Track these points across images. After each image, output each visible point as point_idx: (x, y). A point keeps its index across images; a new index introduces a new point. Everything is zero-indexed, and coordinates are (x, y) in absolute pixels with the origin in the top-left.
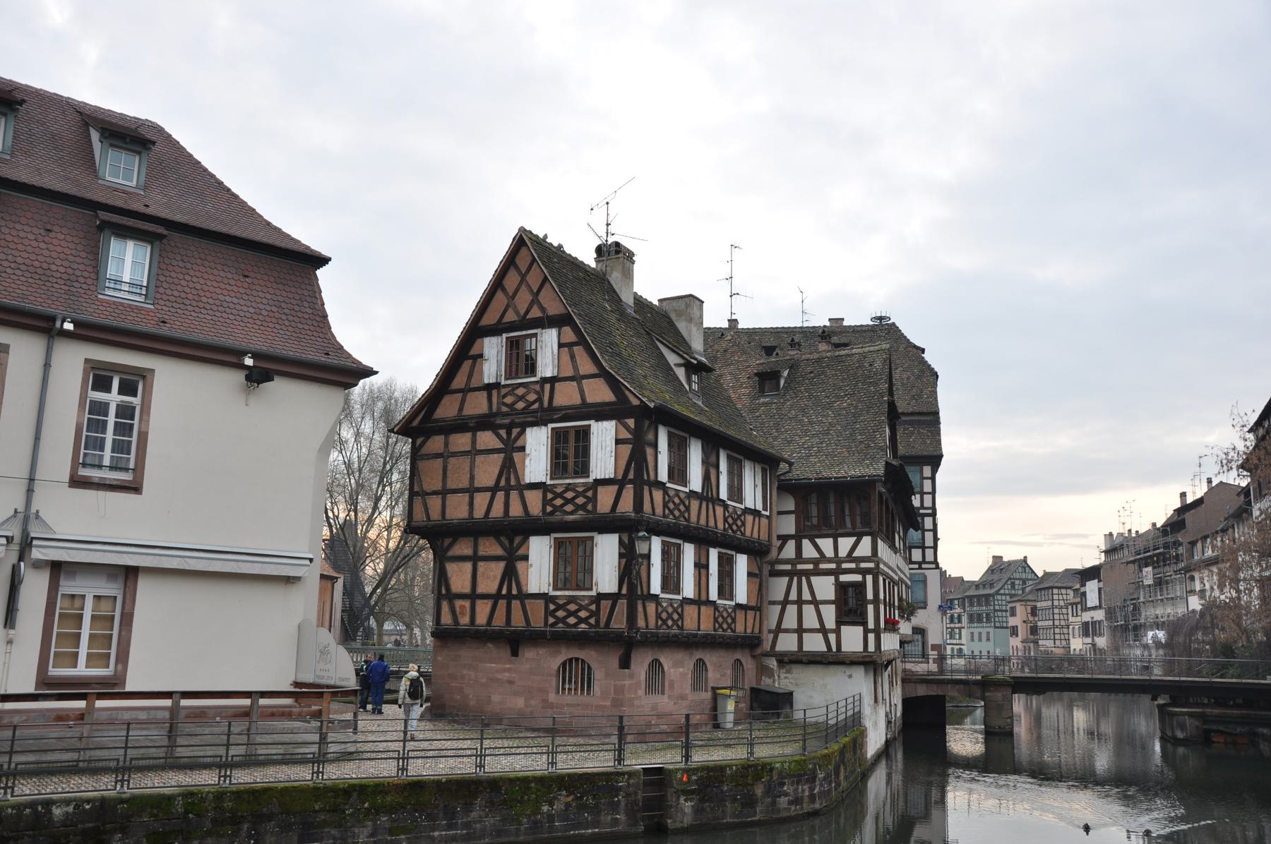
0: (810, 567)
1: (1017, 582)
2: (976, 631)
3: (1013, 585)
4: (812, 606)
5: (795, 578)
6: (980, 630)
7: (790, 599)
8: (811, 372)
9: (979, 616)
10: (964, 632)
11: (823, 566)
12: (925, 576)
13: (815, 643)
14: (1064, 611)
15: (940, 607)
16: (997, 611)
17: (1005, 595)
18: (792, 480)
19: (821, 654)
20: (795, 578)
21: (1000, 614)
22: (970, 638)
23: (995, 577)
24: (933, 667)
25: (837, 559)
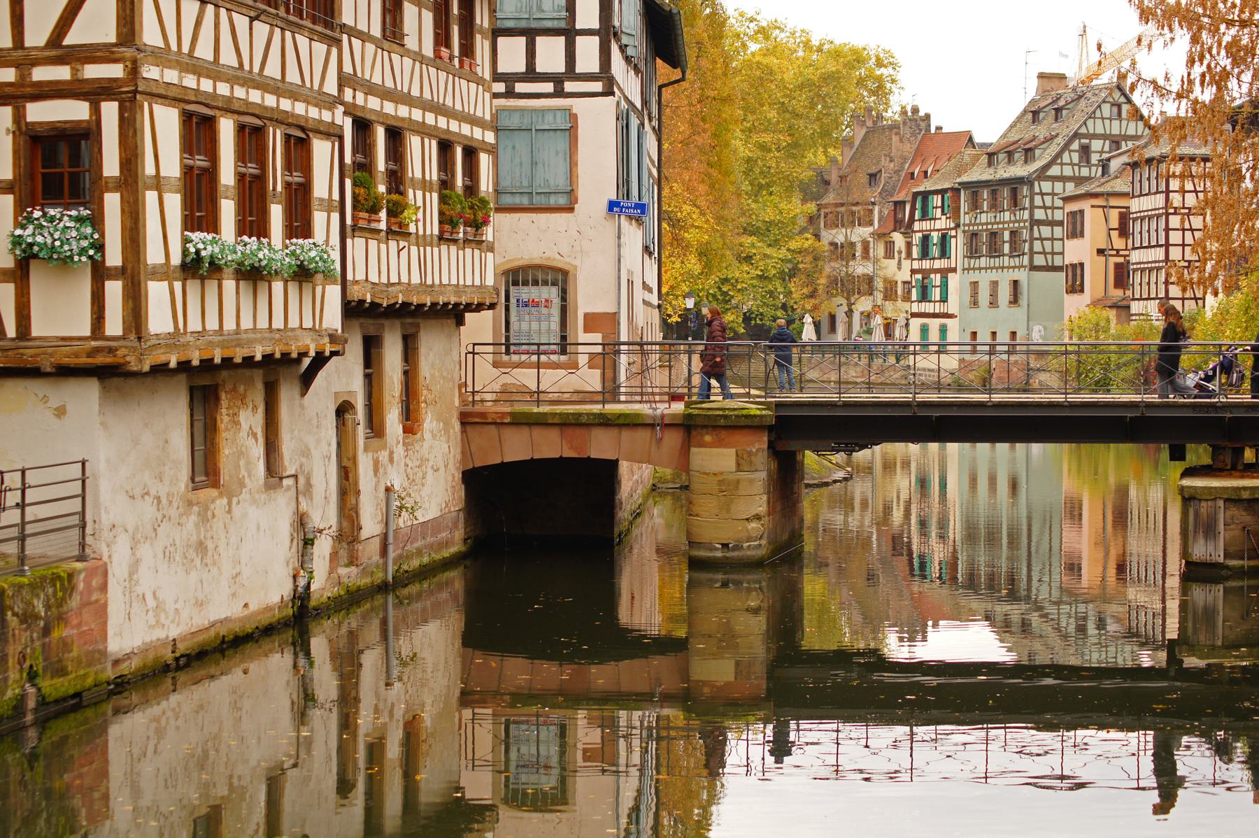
1: (1096, 145)
2: (984, 279)
3: (1085, 151)
6: (994, 275)
9: (993, 235)
10: (953, 280)
12: (574, 118)
15: (612, 205)
16: (1040, 223)
17: (1063, 179)
21: (1046, 231)
23: (1041, 131)
24: (592, 380)
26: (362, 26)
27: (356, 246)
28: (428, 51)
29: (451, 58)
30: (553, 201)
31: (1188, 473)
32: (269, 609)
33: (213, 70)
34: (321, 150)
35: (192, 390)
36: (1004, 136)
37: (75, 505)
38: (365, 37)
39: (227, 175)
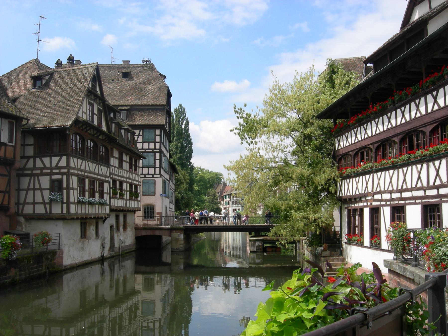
0: (39, 172)
4: (40, 191)
5: (33, 177)
7: (30, 188)
8: (59, 77)
9: (236, 202)
11: (45, 171)
12: (155, 181)
13: (40, 210)
15: (161, 195)
18: (30, 128)
19: (43, 215)
20: (33, 177)
25: (51, 168)
26: (115, 165)
27: (113, 200)
28: (128, 169)
29: (132, 171)
30: (152, 194)
31: (251, 237)
32: (96, 258)
33: (85, 171)
34: (106, 185)
35: (81, 223)
37: (58, 241)
38: (115, 167)
39: (87, 187)
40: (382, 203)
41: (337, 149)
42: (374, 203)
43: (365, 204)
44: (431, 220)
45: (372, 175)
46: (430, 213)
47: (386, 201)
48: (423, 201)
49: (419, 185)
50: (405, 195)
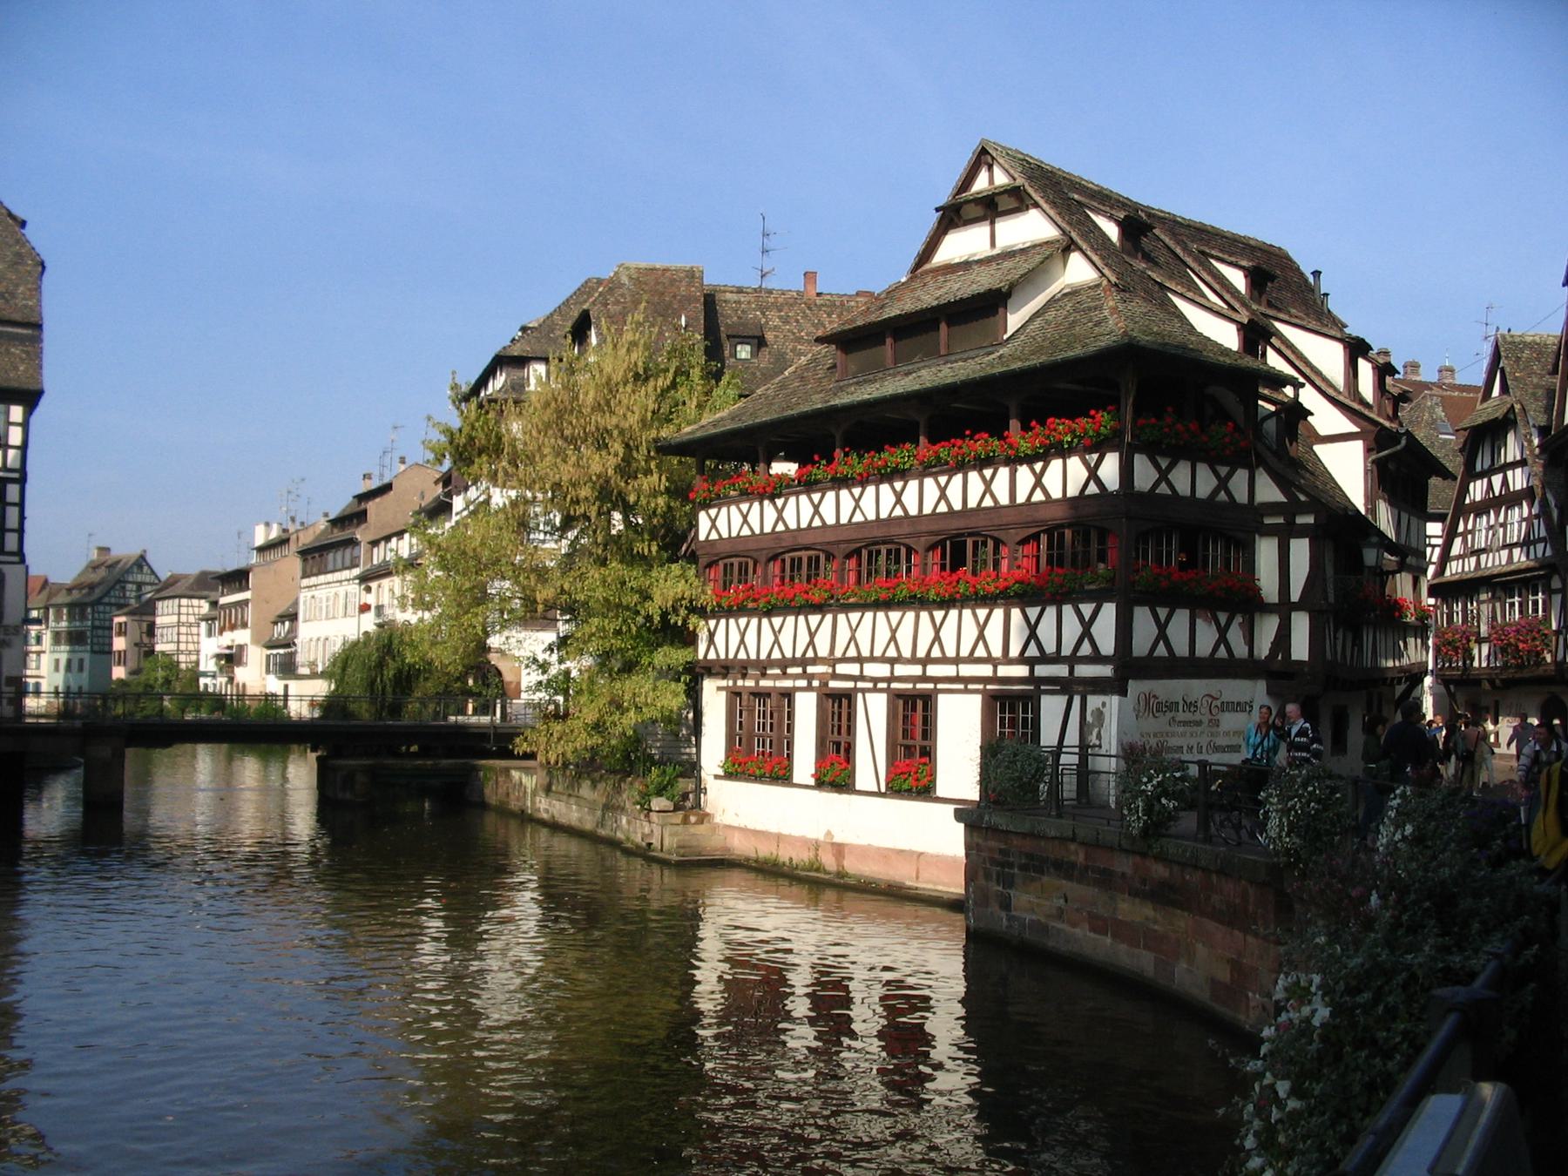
10: (45, 658)
14: (194, 630)
21: (100, 632)
22: (53, 668)
36: (75, 580)
40: (860, 685)
41: (702, 537)
42: (833, 684)
43: (803, 683)
44: (1002, 725)
45: (829, 617)
46: (1003, 711)
47: (875, 680)
48: (989, 687)
49: (980, 652)
50: (933, 670)
